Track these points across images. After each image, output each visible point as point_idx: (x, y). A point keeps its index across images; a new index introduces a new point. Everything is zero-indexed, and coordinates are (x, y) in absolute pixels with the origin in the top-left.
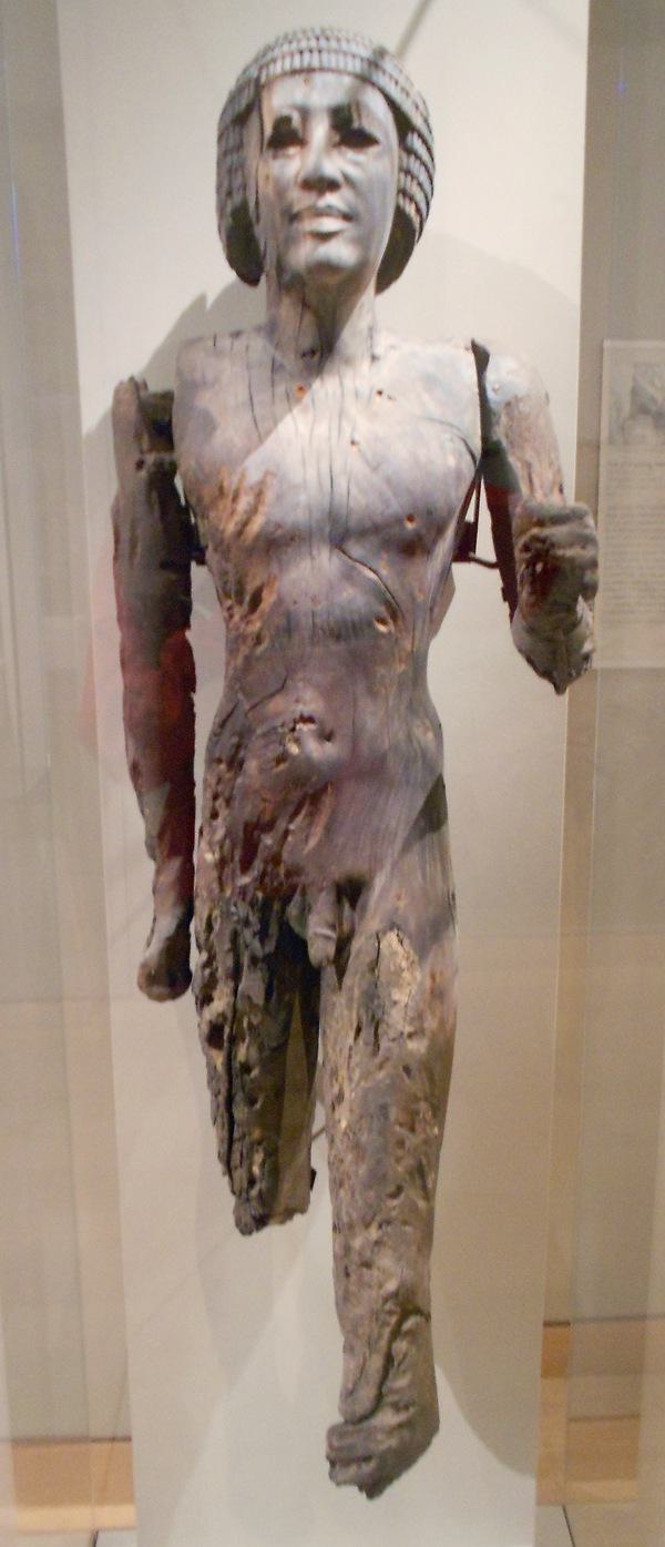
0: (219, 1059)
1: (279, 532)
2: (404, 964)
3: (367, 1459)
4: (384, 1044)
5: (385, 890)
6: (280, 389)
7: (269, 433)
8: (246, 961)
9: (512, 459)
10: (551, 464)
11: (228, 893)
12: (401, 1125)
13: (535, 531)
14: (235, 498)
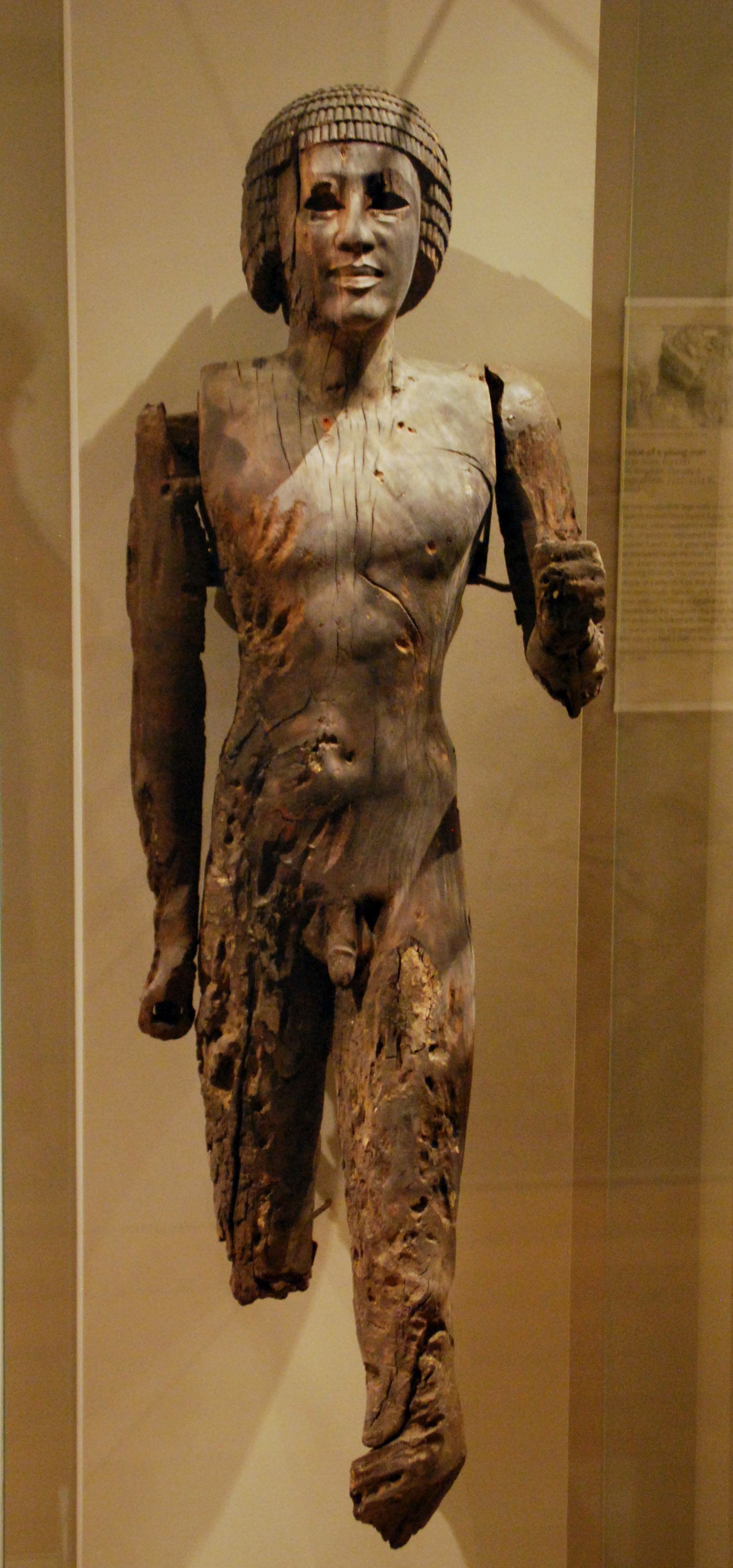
0: (226, 1098)
1: (308, 557)
2: (425, 979)
3: (395, 1477)
4: (407, 1056)
5: (405, 906)
6: (308, 421)
7: (297, 464)
8: (261, 986)
9: (525, 486)
10: (563, 489)
11: (243, 917)
12: (424, 1137)
13: (553, 565)
14: (266, 527)
